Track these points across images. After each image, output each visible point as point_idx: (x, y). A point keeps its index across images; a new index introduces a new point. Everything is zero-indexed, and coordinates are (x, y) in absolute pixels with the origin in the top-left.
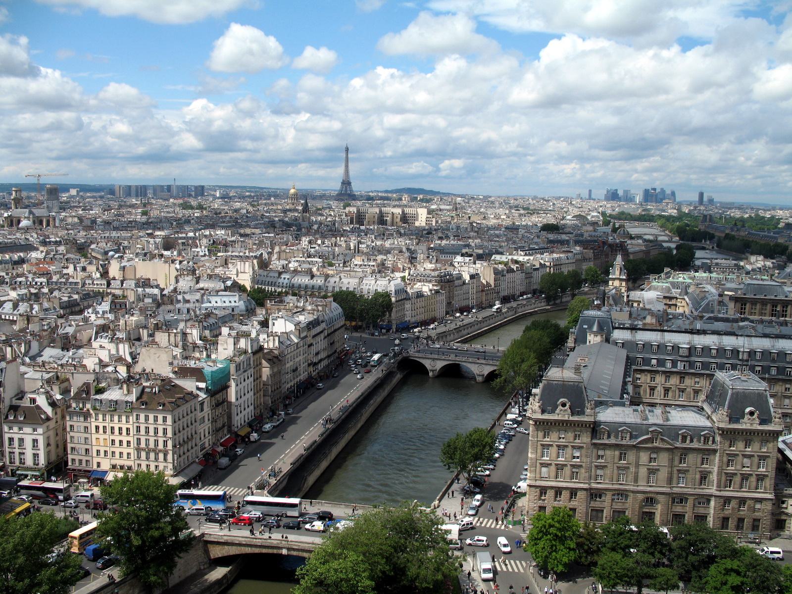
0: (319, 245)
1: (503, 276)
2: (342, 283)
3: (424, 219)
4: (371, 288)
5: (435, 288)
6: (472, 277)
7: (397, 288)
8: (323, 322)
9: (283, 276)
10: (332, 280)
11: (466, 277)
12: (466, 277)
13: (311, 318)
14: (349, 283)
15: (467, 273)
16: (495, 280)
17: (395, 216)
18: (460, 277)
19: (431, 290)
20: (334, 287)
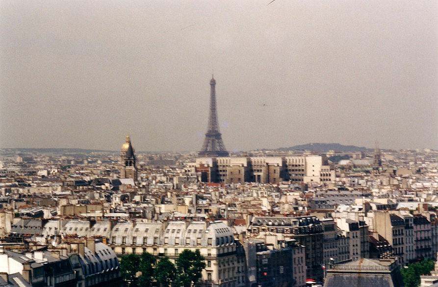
0: (137, 203)
1: (407, 227)
2: (137, 230)
3: (317, 174)
4: (179, 235)
5: (288, 240)
6: (353, 226)
7: (221, 235)
8: (77, 266)
9: (47, 225)
10: (121, 227)
11: (343, 226)
12: (343, 226)
13: (55, 257)
14: (147, 230)
15: (344, 220)
16: (395, 233)
17: (272, 168)
18: (332, 227)
19: (279, 242)
20: (124, 238)
